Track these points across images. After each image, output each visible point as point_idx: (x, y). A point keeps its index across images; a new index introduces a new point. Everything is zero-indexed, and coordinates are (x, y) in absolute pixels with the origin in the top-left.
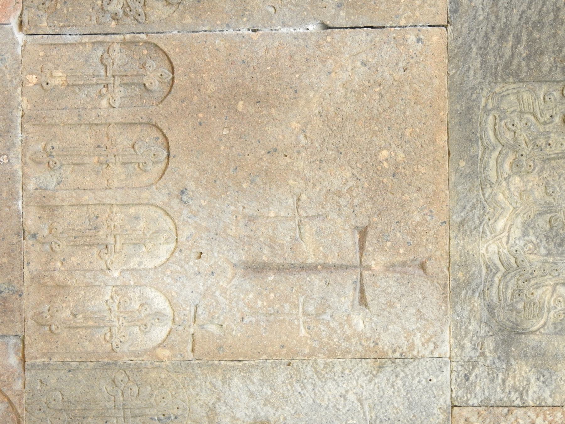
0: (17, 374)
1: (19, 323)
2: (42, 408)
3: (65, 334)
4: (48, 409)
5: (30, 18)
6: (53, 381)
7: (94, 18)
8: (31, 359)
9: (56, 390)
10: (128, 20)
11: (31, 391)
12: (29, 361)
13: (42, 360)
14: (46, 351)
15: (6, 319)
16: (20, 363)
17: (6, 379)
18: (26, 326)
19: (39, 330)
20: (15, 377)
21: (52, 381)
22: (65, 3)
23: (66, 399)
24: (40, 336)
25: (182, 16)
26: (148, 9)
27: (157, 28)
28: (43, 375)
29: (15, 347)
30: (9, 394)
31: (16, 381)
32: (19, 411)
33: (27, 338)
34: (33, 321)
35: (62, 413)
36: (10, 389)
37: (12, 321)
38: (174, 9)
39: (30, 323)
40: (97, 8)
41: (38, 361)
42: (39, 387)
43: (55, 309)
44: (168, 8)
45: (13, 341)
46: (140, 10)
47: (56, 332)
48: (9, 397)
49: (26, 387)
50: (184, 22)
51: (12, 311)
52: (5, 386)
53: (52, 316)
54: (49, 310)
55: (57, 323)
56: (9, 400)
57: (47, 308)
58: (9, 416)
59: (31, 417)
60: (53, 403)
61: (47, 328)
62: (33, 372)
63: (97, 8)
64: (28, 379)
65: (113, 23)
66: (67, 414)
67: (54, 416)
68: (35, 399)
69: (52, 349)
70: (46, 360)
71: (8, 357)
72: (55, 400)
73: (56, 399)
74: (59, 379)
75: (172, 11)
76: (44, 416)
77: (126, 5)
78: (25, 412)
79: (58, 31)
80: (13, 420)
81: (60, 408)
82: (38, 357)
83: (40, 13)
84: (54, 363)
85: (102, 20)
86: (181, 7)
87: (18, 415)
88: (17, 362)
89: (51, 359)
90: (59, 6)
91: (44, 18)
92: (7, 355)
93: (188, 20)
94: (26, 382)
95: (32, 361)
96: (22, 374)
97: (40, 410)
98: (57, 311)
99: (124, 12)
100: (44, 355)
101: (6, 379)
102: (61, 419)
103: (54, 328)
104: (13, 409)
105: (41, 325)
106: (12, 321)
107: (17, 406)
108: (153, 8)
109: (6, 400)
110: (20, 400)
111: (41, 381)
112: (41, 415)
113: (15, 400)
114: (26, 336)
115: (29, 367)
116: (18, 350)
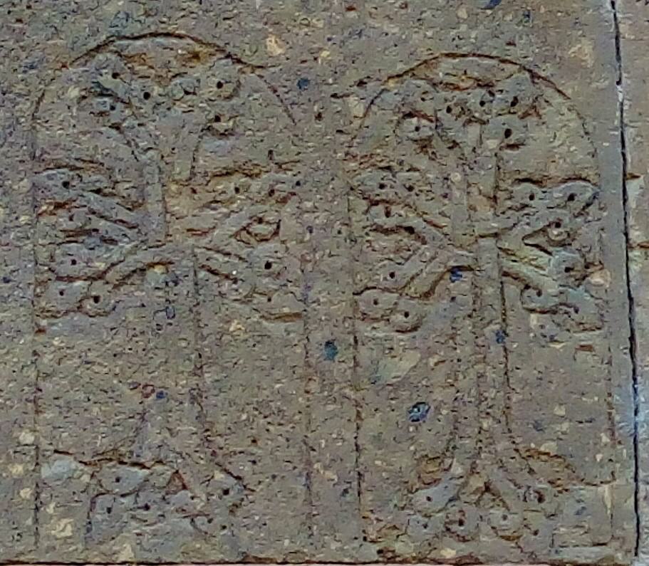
5: (588, 539)
7: (583, 336)
10: (588, 233)
22: (538, 427)
25: (574, 67)
26: (552, 171)
27: (609, 146)
38: (549, 92)
40: (550, 329)
44: (545, 110)
46: (558, 194)
50: (590, 63)
63: (550, 329)
65: (596, 279)
75: (558, 99)
77: (540, 240)
79: (625, 452)
83: (570, 507)
85: (589, 312)
86: (546, 70)
90: (549, 447)
91: (587, 492)
93: (584, 50)
99: (563, 244)
108: (550, 158)
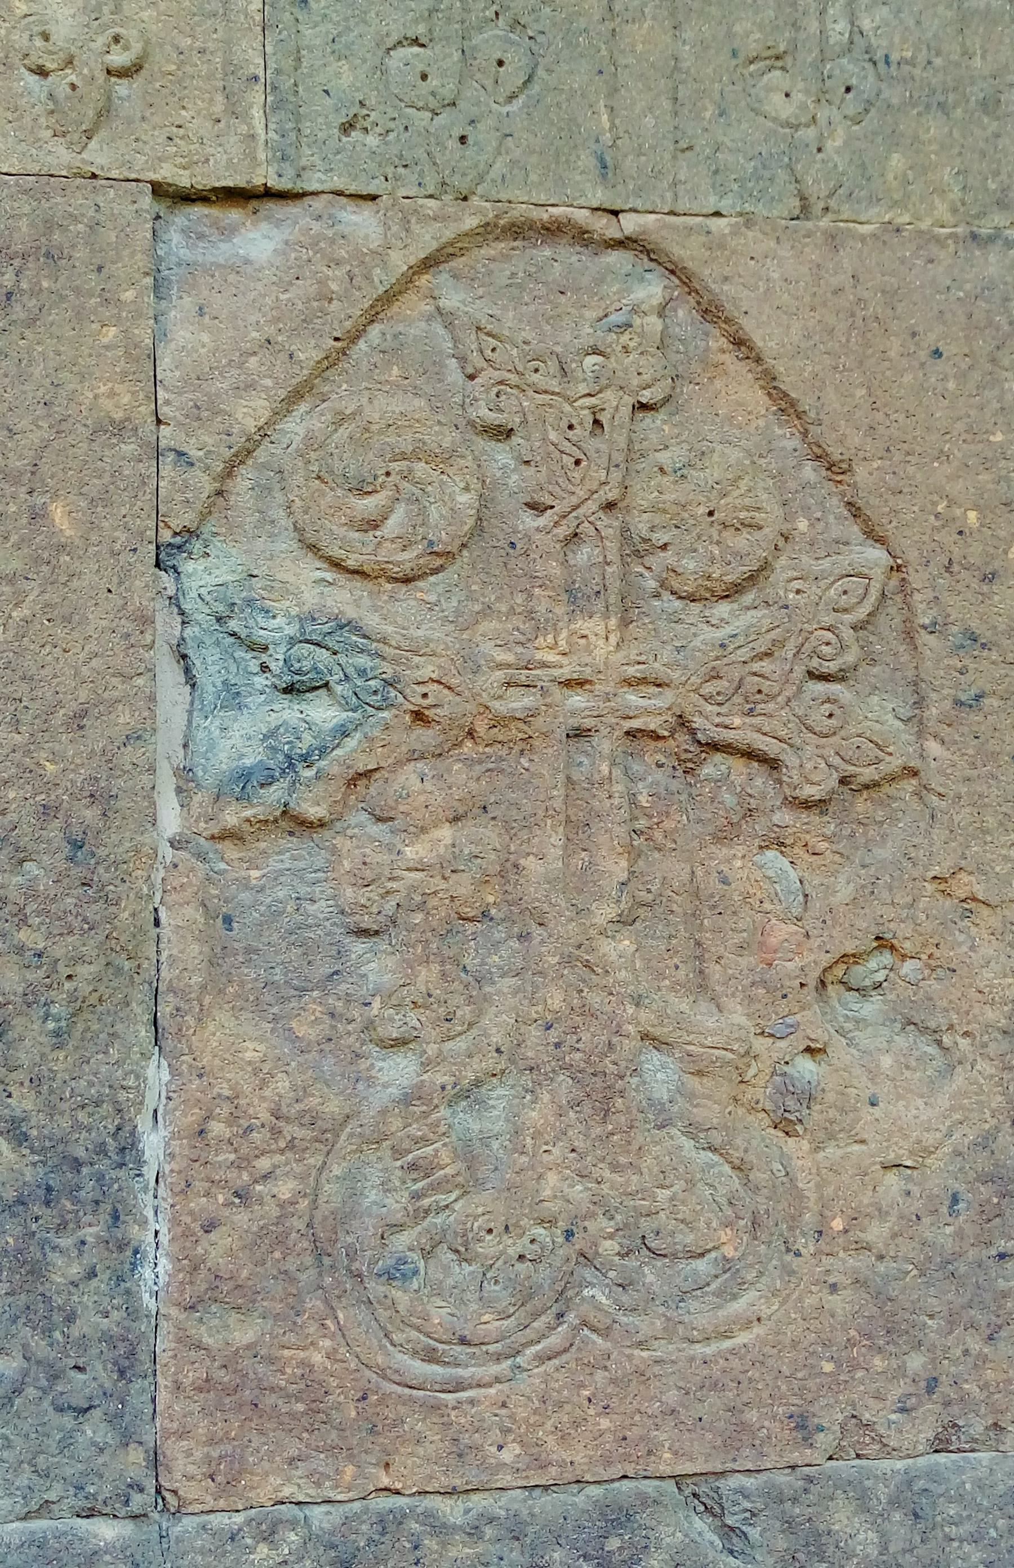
0: (316, 226)
1: (100, 200)
2: (457, 133)
3: (145, 15)
4: (462, 104)
6: (346, 78)
8: (254, 161)
9: (381, 69)
11: (390, 171)
12: (261, 171)
13: (257, 113)
14: (220, 98)
15: (81, 254)
16: (267, 218)
17: (340, 272)
18: (114, 174)
19: (129, 121)
20: (330, 233)
21: (347, 79)
23: (421, 30)
24: (157, 119)
28: (322, 118)
29: (201, 236)
30: (400, 262)
31: (346, 231)
32: (471, 222)
33: (166, 173)
34: (93, 144)
35: (474, 48)
36: (380, 255)
37: (95, 226)
39: (98, 156)
41: (260, 131)
42: (372, 140)
43: (39, 42)
45: (175, 242)
47: (137, 48)
48: (413, 260)
49: (372, 190)
51: (50, 225)
52: (368, 277)
53: (70, 62)
54: (42, 72)
55: (101, 41)
56: (429, 264)
57: (32, 79)
58: (490, 273)
59: (492, 174)
60: (433, 82)
61: (122, 88)
62: (308, 155)
64: (338, 182)
66: (480, 29)
67: (489, 83)
68: (420, 153)
69: (210, 76)
70: (257, 96)
71: (247, 262)
72: (424, 77)
73: (421, 67)
74: (338, 49)
76: (491, 122)
78: (475, 201)
80: (506, 258)
81: (457, 56)
82: (244, 129)
84: (272, 65)
87: (487, 232)
88: (264, 226)
89: (256, 78)
92: (240, 267)
94: (352, 189)
95: (262, 156)
96: (317, 204)
97: (463, 139)
98: (46, 37)
100: (235, 111)
101: (340, 272)
102: (498, 55)
103: (119, 58)
104: (462, 252)
105: (105, 113)
106: (95, 226)
107: (449, 234)
109: (423, 281)
110: (425, 219)
111: (347, 128)
112: (483, 135)
113: (427, 239)
114: (156, 177)
115: (290, 172)
116: (215, 224)
